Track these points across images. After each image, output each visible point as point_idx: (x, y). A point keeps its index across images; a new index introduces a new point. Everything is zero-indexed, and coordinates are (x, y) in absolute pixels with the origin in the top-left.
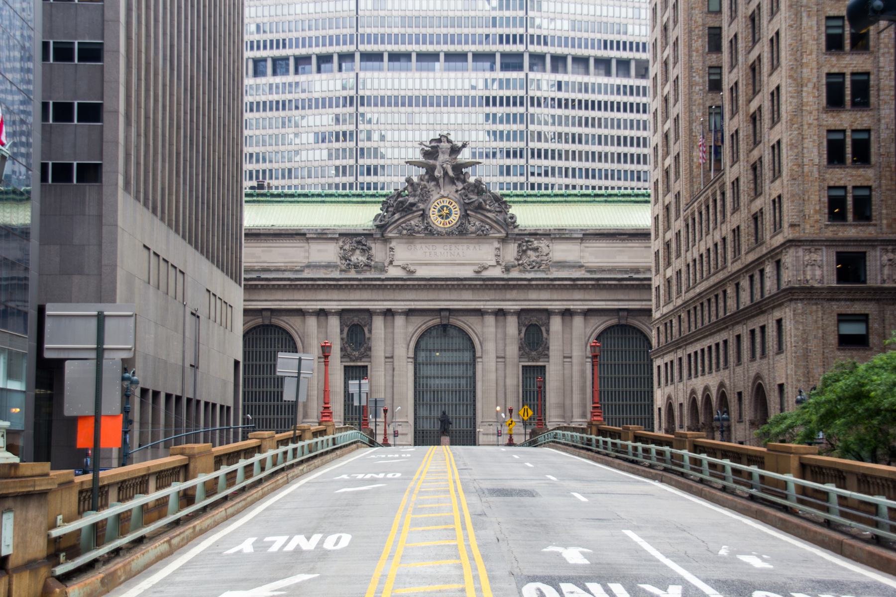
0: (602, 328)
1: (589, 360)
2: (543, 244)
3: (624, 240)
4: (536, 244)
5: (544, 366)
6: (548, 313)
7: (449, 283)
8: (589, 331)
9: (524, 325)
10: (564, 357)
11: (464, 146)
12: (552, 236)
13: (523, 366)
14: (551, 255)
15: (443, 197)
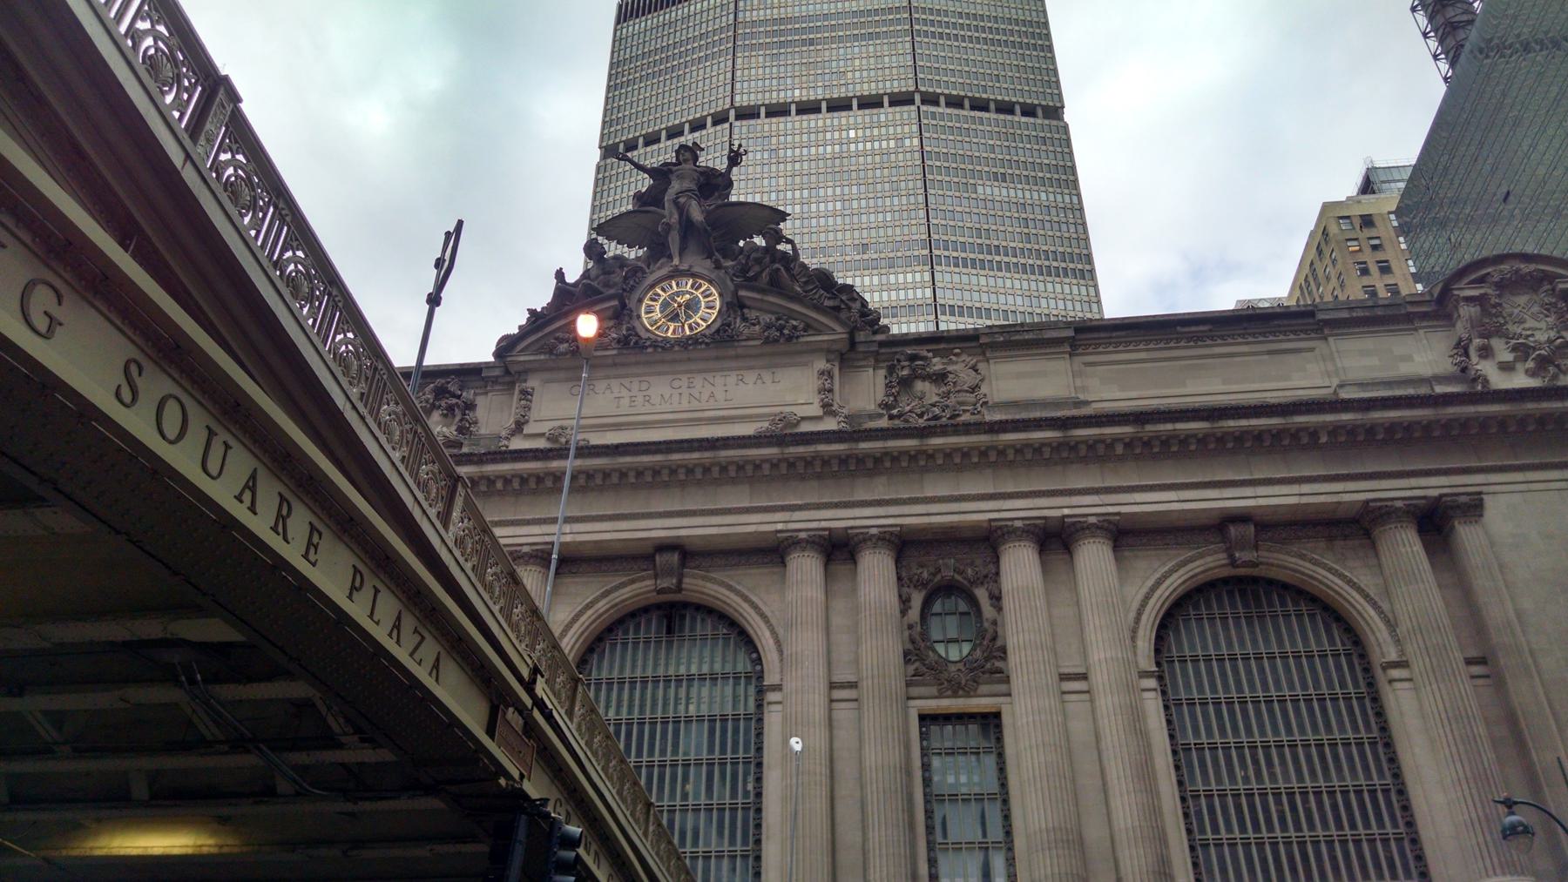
0: (1175, 583)
1: (1152, 683)
2: (960, 368)
3: (1200, 338)
4: (937, 364)
5: (997, 715)
6: (990, 540)
7: (676, 457)
8: (1135, 592)
9: (920, 584)
10: (1064, 677)
11: (735, 158)
12: (983, 340)
13: (924, 718)
14: (984, 389)
15: (676, 274)
